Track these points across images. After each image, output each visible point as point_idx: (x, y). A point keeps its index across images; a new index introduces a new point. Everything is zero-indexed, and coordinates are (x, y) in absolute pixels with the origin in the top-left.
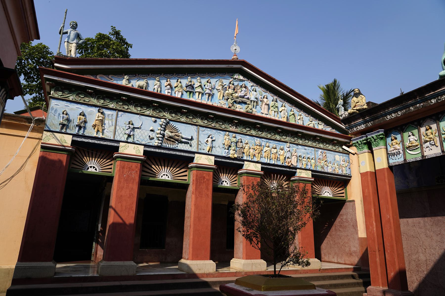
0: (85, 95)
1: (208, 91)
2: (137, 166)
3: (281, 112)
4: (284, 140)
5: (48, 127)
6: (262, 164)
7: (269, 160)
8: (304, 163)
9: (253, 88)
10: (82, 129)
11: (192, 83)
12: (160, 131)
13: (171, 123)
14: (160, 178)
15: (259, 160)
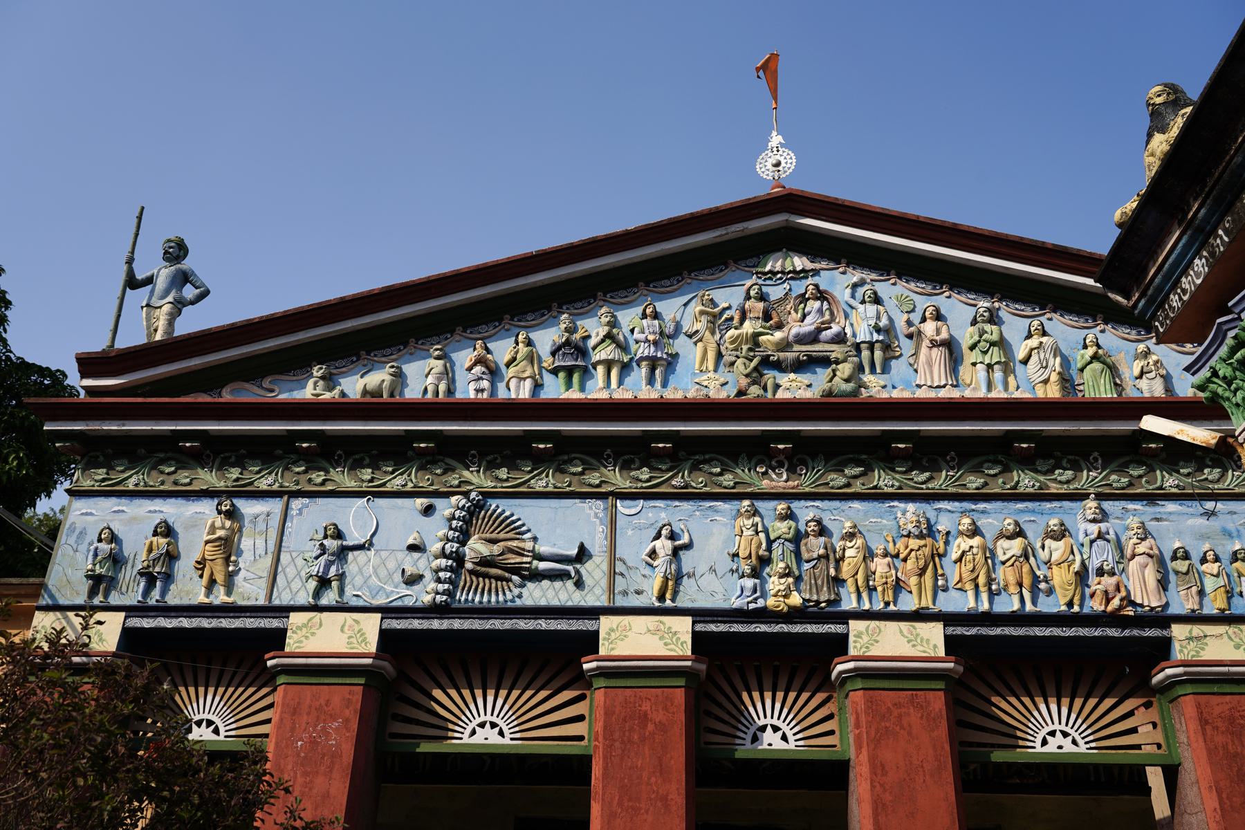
0: (178, 461)
1: (644, 350)
2: (347, 699)
3: (1025, 362)
4: (1063, 490)
5: (52, 596)
6: (949, 619)
7: (984, 596)
8: (1210, 584)
9: (861, 291)
10: (158, 583)
11: (577, 336)
12: (439, 545)
13: (493, 503)
14: (466, 739)
15: (927, 602)
